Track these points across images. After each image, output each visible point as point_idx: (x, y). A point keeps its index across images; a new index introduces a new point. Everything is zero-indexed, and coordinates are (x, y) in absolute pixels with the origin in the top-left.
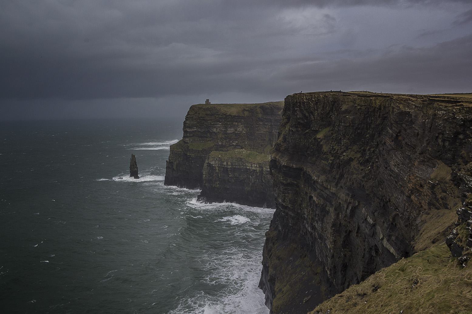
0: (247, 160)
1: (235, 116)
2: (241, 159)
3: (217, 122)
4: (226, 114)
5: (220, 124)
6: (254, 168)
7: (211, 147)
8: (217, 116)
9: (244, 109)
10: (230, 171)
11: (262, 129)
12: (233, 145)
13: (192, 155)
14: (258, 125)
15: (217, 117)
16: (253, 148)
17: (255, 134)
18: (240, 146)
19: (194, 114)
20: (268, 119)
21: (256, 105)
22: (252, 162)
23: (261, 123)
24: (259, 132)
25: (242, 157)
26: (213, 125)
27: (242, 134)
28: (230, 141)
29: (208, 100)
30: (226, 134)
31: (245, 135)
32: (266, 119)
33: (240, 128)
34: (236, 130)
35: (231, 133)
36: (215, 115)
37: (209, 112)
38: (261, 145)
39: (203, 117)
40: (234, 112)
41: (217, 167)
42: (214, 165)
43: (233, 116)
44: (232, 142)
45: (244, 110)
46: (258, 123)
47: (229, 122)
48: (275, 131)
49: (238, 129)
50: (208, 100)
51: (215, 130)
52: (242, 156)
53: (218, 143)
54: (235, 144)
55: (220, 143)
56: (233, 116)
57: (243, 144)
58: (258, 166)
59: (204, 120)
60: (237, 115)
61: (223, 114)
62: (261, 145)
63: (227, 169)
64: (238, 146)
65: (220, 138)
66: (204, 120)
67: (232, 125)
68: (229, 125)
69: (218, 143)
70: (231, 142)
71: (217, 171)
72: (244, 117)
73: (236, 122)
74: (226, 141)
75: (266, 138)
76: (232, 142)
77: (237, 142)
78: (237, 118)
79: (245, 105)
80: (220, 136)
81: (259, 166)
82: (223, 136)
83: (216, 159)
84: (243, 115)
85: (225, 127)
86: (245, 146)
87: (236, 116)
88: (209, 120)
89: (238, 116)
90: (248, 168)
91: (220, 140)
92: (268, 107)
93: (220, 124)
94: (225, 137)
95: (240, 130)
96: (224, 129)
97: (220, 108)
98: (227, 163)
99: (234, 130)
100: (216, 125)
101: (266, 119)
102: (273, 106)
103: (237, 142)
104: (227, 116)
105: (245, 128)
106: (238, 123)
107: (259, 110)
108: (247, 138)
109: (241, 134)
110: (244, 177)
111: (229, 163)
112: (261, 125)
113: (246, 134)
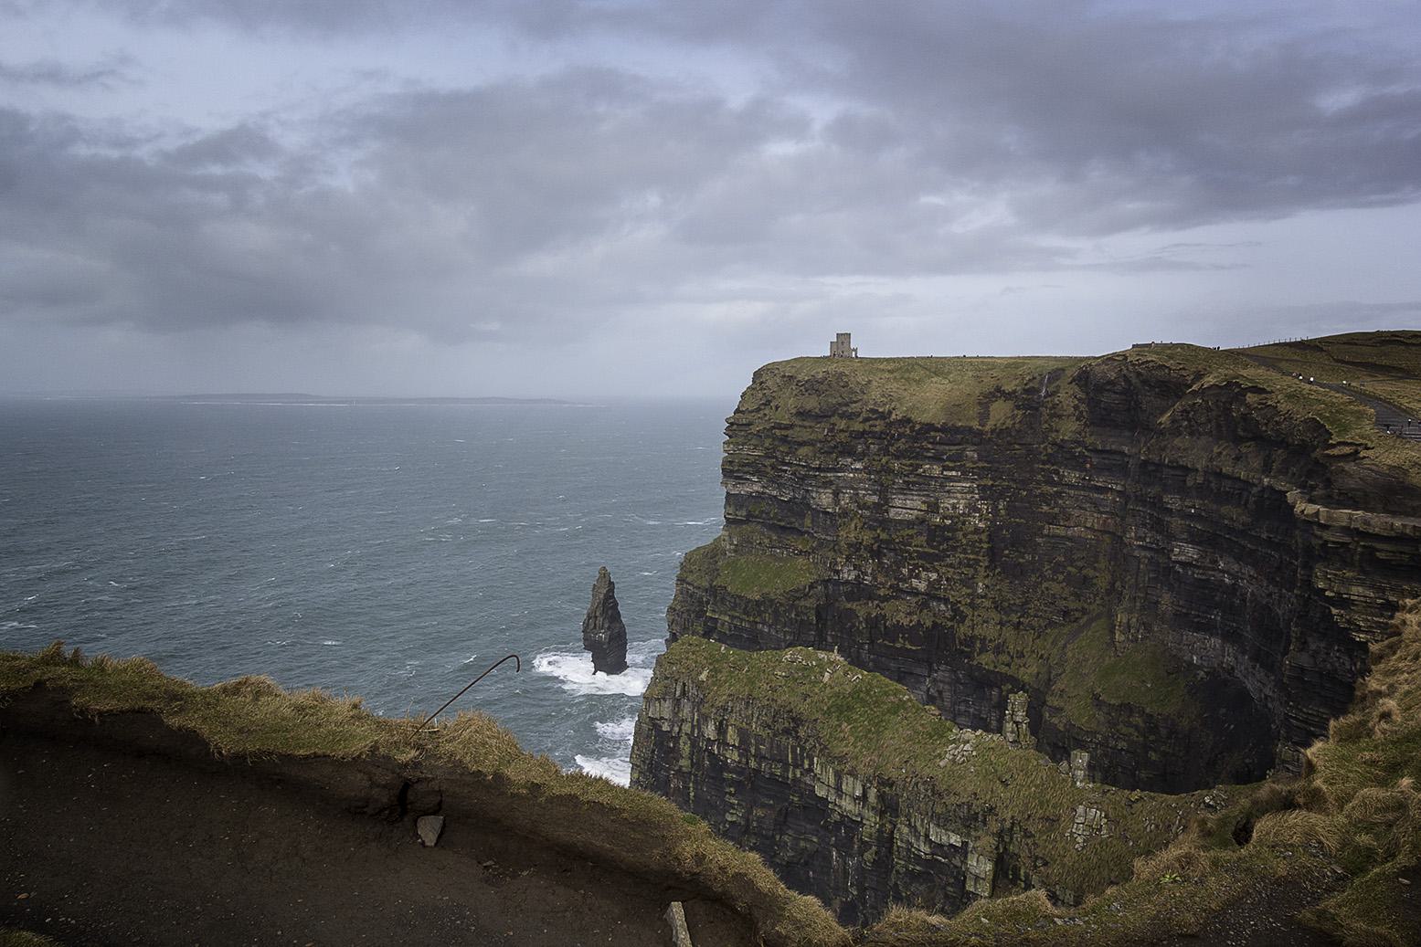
0: (825, 733)
1: (930, 427)
2: (797, 721)
3: (843, 454)
5: (858, 466)
6: (847, 804)
7: (797, 591)
8: (842, 424)
9: (998, 389)
10: (737, 784)
11: (1076, 512)
12: (914, 592)
13: (722, 617)
14: (1053, 484)
15: (842, 431)
16: (1017, 626)
17: (1039, 540)
18: (946, 601)
19: (758, 410)
20: (1107, 452)
21: (1057, 371)
22: (841, 759)
23: (1072, 476)
24: (1060, 531)
25: (803, 708)
26: (818, 469)
27: (965, 535)
28: (899, 565)
29: (844, 338)
30: (885, 524)
31: (981, 541)
32: (1096, 451)
33: (959, 498)
34: (933, 508)
35: (910, 524)
36: (833, 420)
37: (811, 403)
38: (1066, 613)
39: (787, 428)
40: (929, 402)
41: (684, 738)
42: (665, 728)
45: (998, 393)
46: (1057, 472)
47: (898, 458)
48: (1140, 539)
49: (947, 503)
50: (844, 338)
51: (824, 499)
52: (806, 696)
53: (837, 572)
54: (922, 586)
55: (849, 574)
56: (917, 427)
57: (965, 591)
58: (872, 798)
59: (784, 440)
60: (940, 420)
61: (873, 411)
62: (1066, 613)
63: (719, 766)
64: (939, 599)
65: (850, 545)
66: (784, 440)
67: (912, 479)
68: (900, 474)
69: (837, 572)
70: (905, 571)
71: (684, 763)
72: (980, 433)
73: (937, 459)
74: (880, 563)
75: (1095, 569)
77: (934, 576)
78: (938, 436)
79: (982, 366)
80: (850, 533)
81: (881, 797)
82: (867, 537)
83: (684, 693)
84: (975, 425)
85: (882, 485)
86: (972, 606)
87: (937, 430)
88: (802, 444)
89: (943, 429)
90: (820, 793)
91: (848, 558)
92: (1112, 375)
93: (858, 466)
94: (877, 539)
95: (954, 507)
96: (875, 498)
97: (870, 382)
98: (721, 730)
99: (924, 507)
100: (834, 470)
101: (1096, 451)
102: (1139, 374)
103: (934, 576)
104: (892, 423)
105: (982, 498)
106: (946, 468)
107: (1067, 396)
108: (991, 561)
109: (960, 534)
110: (802, 844)
111: (732, 736)
112: (1071, 486)
113: (984, 537)
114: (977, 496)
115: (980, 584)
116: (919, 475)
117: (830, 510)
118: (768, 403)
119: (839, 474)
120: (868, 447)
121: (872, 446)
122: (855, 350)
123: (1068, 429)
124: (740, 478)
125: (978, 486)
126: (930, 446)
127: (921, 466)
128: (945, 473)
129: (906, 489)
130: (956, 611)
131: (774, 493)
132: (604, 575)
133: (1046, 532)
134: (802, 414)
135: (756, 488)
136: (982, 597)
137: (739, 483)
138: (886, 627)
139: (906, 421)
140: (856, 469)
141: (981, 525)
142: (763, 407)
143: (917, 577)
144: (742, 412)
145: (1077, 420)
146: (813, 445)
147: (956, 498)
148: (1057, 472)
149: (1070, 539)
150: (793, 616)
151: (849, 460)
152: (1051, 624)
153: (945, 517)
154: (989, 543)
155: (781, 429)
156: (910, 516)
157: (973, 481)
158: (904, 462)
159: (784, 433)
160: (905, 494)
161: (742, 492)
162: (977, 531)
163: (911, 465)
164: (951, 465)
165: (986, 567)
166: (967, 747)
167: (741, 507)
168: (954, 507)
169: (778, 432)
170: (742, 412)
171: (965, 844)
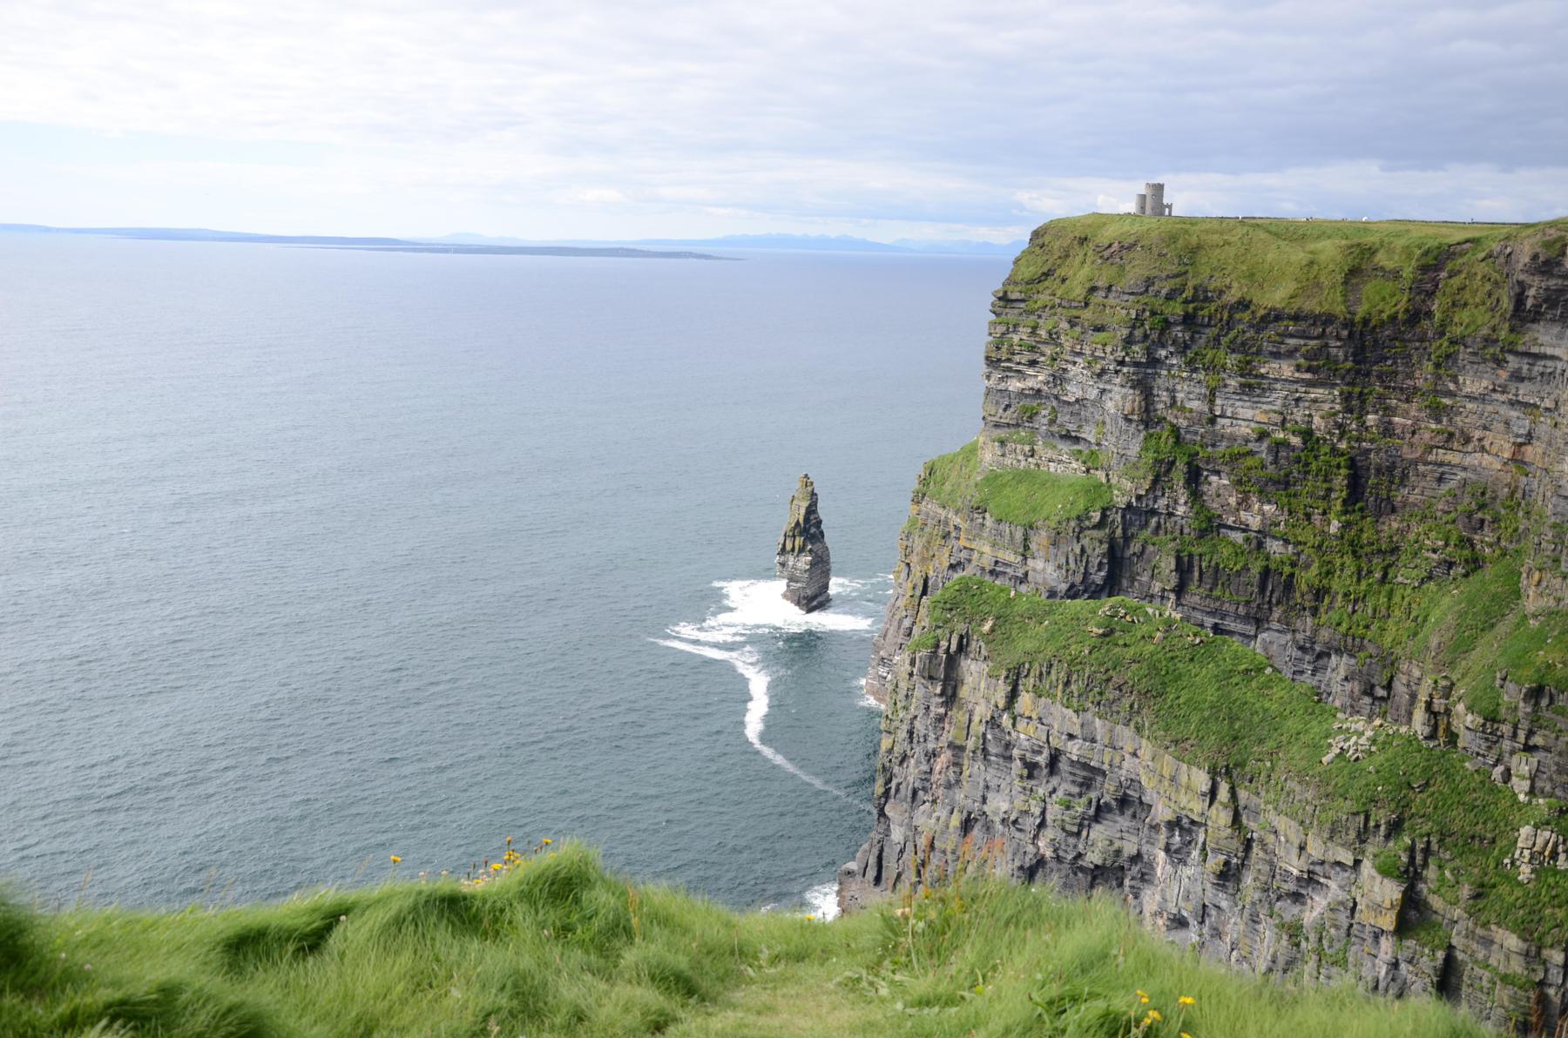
4: (1221, 292)
56: (1262, 312)
116: (1262, 376)
122: (1170, 207)
124: (1010, 370)
125: (1341, 394)
139: (1243, 304)
141: (1343, 445)
148: (1455, 379)
156: (1244, 430)
166: (1363, 741)
171: (1357, 863)
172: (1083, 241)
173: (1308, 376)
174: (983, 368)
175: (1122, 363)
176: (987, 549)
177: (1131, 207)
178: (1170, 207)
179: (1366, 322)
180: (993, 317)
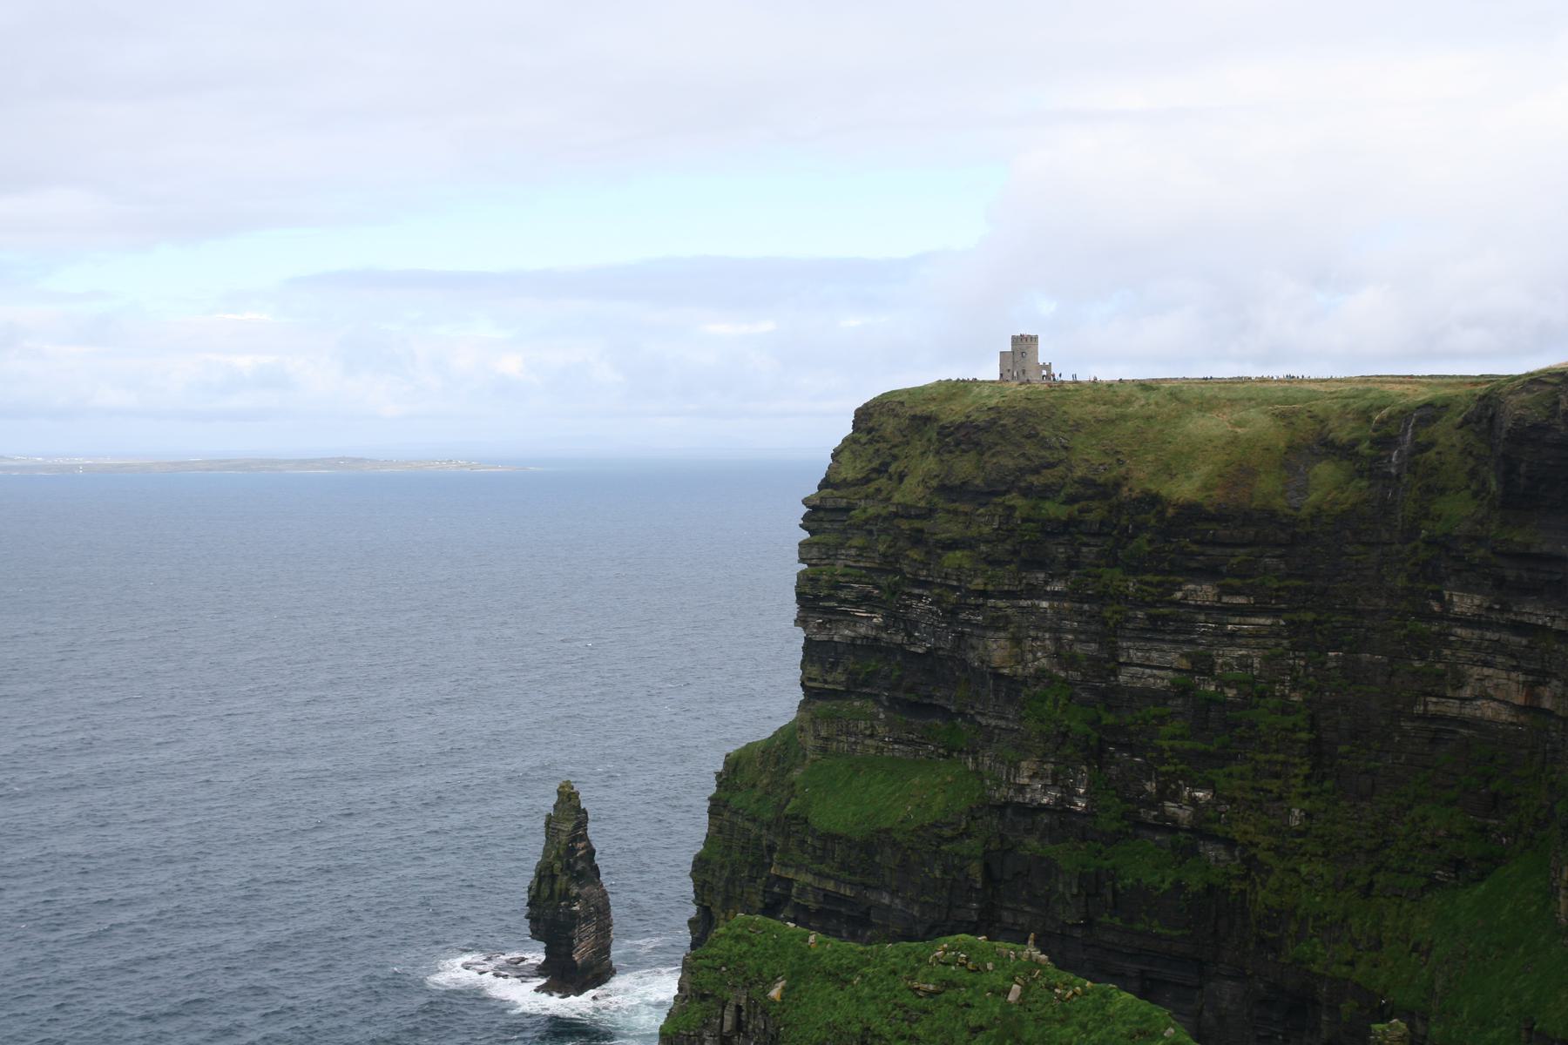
1: (1191, 513)
4: (1117, 485)
12: (1170, 826)
14: (1431, 617)
17: (1407, 725)
19: (867, 480)
29: (1023, 346)
34: (1203, 665)
35: (1159, 697)
37: (964, 467)
38: (1458, 865)
43: (1171, 512)
44: (1163, 794)
45: (1327, 447)
46: (1438, 596)
50: (1023, 346)
51: (997, 649)
54: (1184, 814)
56: (1171, 512)
59: (917, 539)
61: (1085, 482)
62: (1458, 865)
64: (1212, 838)
70: (1150, 787)
73: (1210, 572)
76: (1163, 794)
88: (952, 545)
99: (1185, 664)
114: (1285, 643)
115: (1297, 812)
116: (1178, 604)
117: (1006, 671)
118: (882, 470)
119: (1023, 603)
120: (1078, 552)
121: (1084, 549)
123: (1457, 510)
124: (832, 610)
125: (1291, 623)
126: (1195, 548)
127: (1179, 587)
128: (1225, 599)
129: (1155, 629)
130: (1250, 862)
131: (898, 639)
132: (568, 799)
133: (1419, 709)
134: (950, 490)
135: (862, 631)
136: (1300, 834)
137: (830, 621)
138: (1115, 893)
140: (1055, 593)
142: (874, 476)
143: (1175, 797)
144: (835, 486)
145: (1475, 495)
146: (971, 547)
147: (1247, 646)
148: (1438, 596)
149: (1465, 723)
150: (938, 874)
151: (1041, 576)
152: (1433, 883)
153: (1224, 683)
154: (1310, 732)
155: (909, 517)
156: (1160, 680)
157: (1276, 613)
158: (1148, 578)
159: (917, 524)
160: (1149, 640)
161: (836, 638)
162: (1286, 709)
163: (1160, 584)
164: (1237, 582)
165: (1307, 777)
167: (834, 666)
168: (1244, 664)
169: (905, 525)
170: (835, 486)
172: (928, 419)
173: (1241, 600)
174: (793, 609)
175: (984, 594)
176: (809, 878)
177: (990, 372)
178: (1048, 367)
179: (1314, 518)
180: (806, 535)
